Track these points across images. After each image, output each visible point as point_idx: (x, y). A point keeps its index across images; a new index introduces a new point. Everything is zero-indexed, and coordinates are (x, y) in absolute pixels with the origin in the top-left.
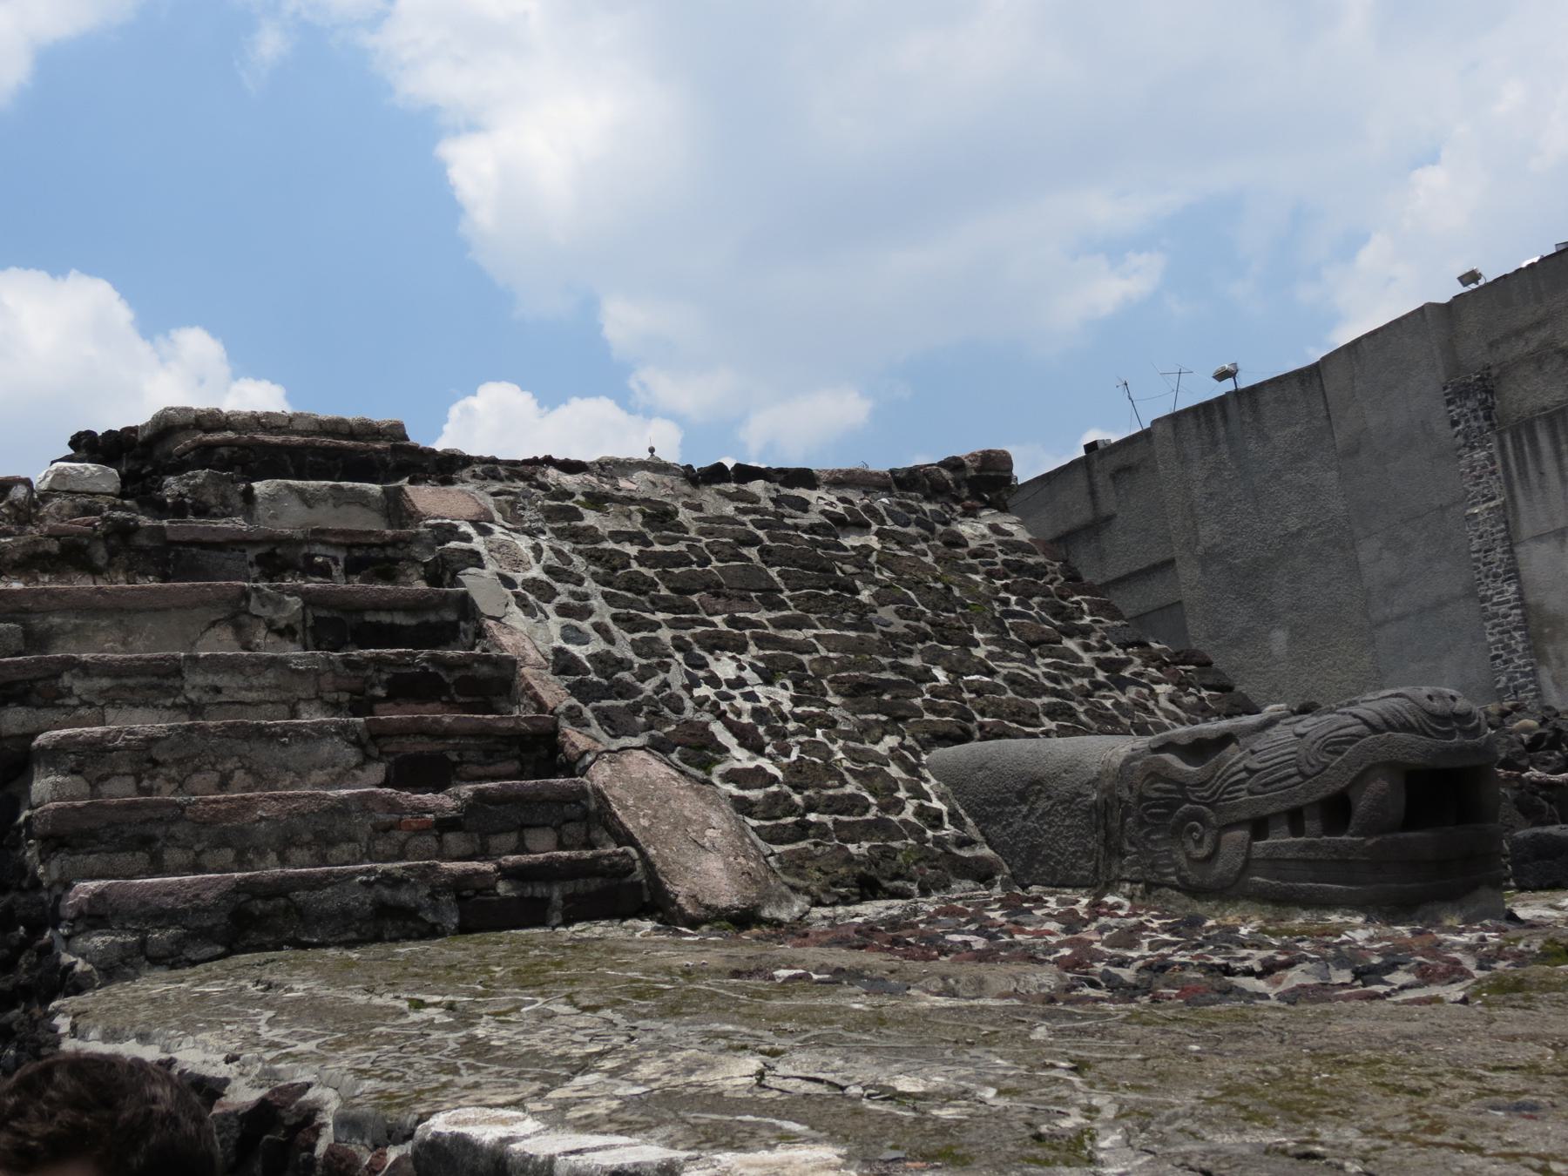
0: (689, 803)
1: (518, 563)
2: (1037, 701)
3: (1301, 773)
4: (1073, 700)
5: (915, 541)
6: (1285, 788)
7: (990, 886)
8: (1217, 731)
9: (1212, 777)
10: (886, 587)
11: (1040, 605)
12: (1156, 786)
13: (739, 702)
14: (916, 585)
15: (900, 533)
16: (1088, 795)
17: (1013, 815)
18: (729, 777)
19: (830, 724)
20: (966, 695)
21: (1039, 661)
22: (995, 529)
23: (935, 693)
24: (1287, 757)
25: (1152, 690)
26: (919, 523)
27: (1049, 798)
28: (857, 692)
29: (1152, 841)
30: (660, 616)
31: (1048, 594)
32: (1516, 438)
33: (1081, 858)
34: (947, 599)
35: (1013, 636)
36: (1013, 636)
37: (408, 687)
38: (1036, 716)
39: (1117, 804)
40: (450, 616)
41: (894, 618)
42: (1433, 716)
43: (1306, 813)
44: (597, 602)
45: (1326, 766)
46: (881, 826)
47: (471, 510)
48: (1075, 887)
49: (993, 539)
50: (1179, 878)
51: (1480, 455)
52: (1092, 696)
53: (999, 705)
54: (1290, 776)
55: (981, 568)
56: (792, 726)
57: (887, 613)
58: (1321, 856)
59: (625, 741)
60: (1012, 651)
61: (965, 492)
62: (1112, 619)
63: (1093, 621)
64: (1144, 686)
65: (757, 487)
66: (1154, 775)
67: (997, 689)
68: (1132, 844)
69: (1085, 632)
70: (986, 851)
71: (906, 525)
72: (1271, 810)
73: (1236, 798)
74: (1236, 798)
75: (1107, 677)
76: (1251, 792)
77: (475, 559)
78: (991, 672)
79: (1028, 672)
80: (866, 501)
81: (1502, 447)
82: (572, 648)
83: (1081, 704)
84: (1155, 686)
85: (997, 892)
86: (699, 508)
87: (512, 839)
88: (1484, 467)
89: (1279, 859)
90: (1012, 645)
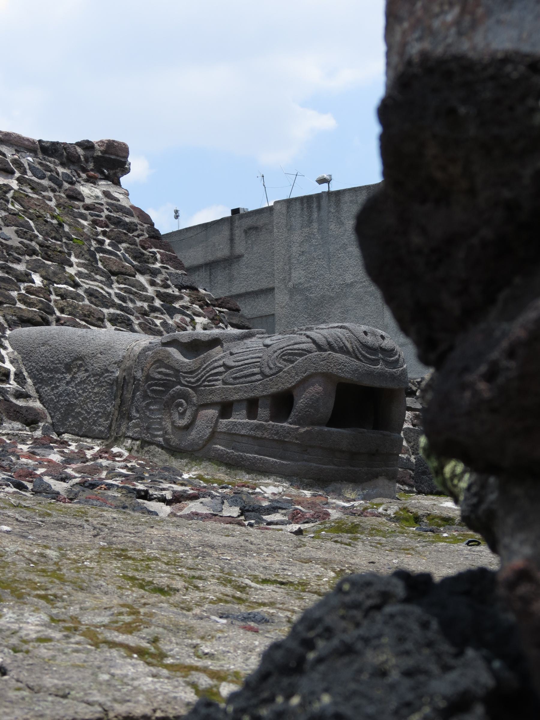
2: (105, 311)
3: (262, 373)
4: (133, 315)
5: (45, 189)
6: (249, 382)
7: (35, 429)
8: (209, 335)
9: (199, 368)
10: (14, 214)
11: (126, 250)
12: (160, 370)
14: (37, 218)
15: (35, 182)
16: (113, 372)
17: (60, 380)
20: (53, 297)
21: (115, 285)
22: (107, 194)
23: (29, 291)
24: (254, 360)
25: (193, 320)
26: (51, 179)
27: (86, 371)
29: (150, 410)
31: (134, 243)
33: (101, 417)
34: (57, 232)
35: (100, 265)
36: (100, 265)
38: (102, 320)
39: (132, 381)
41: (14, 236)
42: (365, 346)
43: (260, 402)
45: (281, 370)
48: (94, 438)
49: (104, 200)
50: (164, 440)
52: (148, 315)
53: (75, 308)
54: (254, 374)
55: (90, 218)
58: (266, 435)
60: (96, 274)
61: (91, 165)
62: (176, 268)
63: (162, 267)
64: (188, 315)
66: (159, 362)
67: (77, 297)
68: (137, 411)
69: (154, 273)
70: (38, 405)
71: (43, 177)
72: (236, 397)
73: (213, 385)
74: (213, 385)
75: (162, 305)
76: (225, 383)
78: (76, 285)
79: (105, 290)
80: (16, 157)
83: (138, 318)
84: (195, 318)
85: (38, 433)
89: (235, 434)
90: (98, 271)
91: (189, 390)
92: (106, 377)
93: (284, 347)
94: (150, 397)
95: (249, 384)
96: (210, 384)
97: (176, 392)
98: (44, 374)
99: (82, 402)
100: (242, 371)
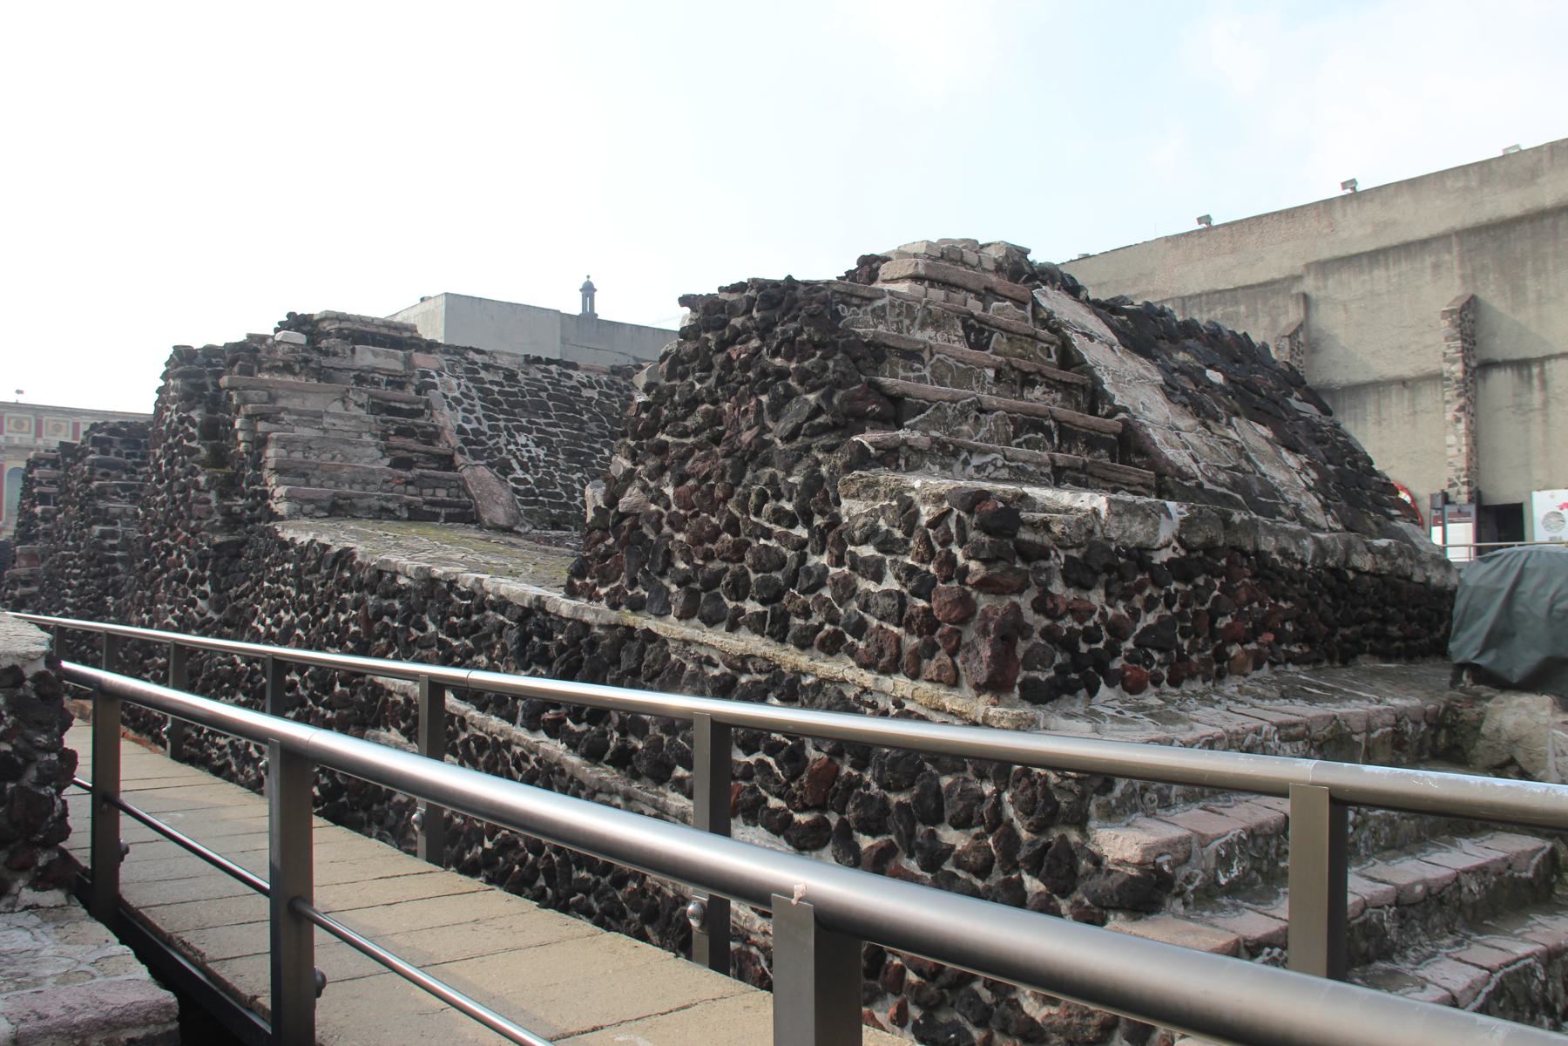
0: (496, 487)
1: (450, 390)
13: (525, 453)
14: (607, 416)
18: (514, 480)
19: (557, 465)
26: (618, 390)
28: (572, 455)
30: (501, 416)
37: (400, 432)
40: (422, 407)
44: (478, 408)
46: (566, 505)
47: (437, 366)
56: (542, 464)
57: (592, 425)
59: (478, 462)
65: (553, 368)
77: (434, 386)
82: (465, 425)
86: (527, 374)
87: (431, 491)
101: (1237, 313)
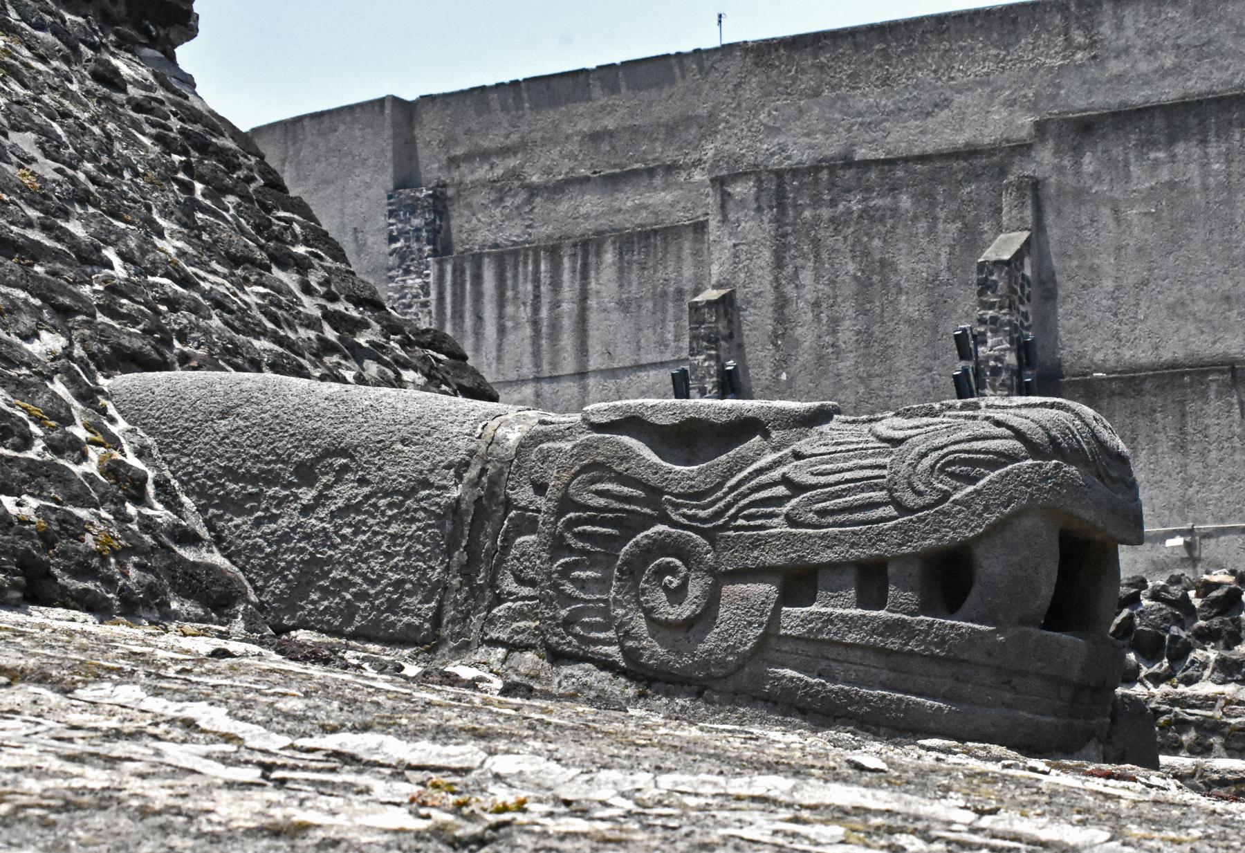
4: (303, 357)
8: (730, 411)
12: (600, 486)
16: (445, 488)
17: (280, 502)
24: (868, 473)
25: (398, 375)
27: (363, 482)
29: (576, 581)
32: (458, 272)
33: (410, 594)
43: (891, 570)
45: (945, 496)
50: (626, 652)
51: (414, 282)
62: (335, 259)
66: (598, 469)
72: (827, 556)
76: (791, 521)
81: (441, 279)
88: (415, 297)
89: (830, 643)
91: (694, 536)
92: (422, 500)
93: (946, 446)
94: (571, 550)
95: (864, 528)
96: (752, 523)
97: (655, 540)
98: (231, 486)
99: (353, 555)
100: (839, 497)
101: (895, 211)
